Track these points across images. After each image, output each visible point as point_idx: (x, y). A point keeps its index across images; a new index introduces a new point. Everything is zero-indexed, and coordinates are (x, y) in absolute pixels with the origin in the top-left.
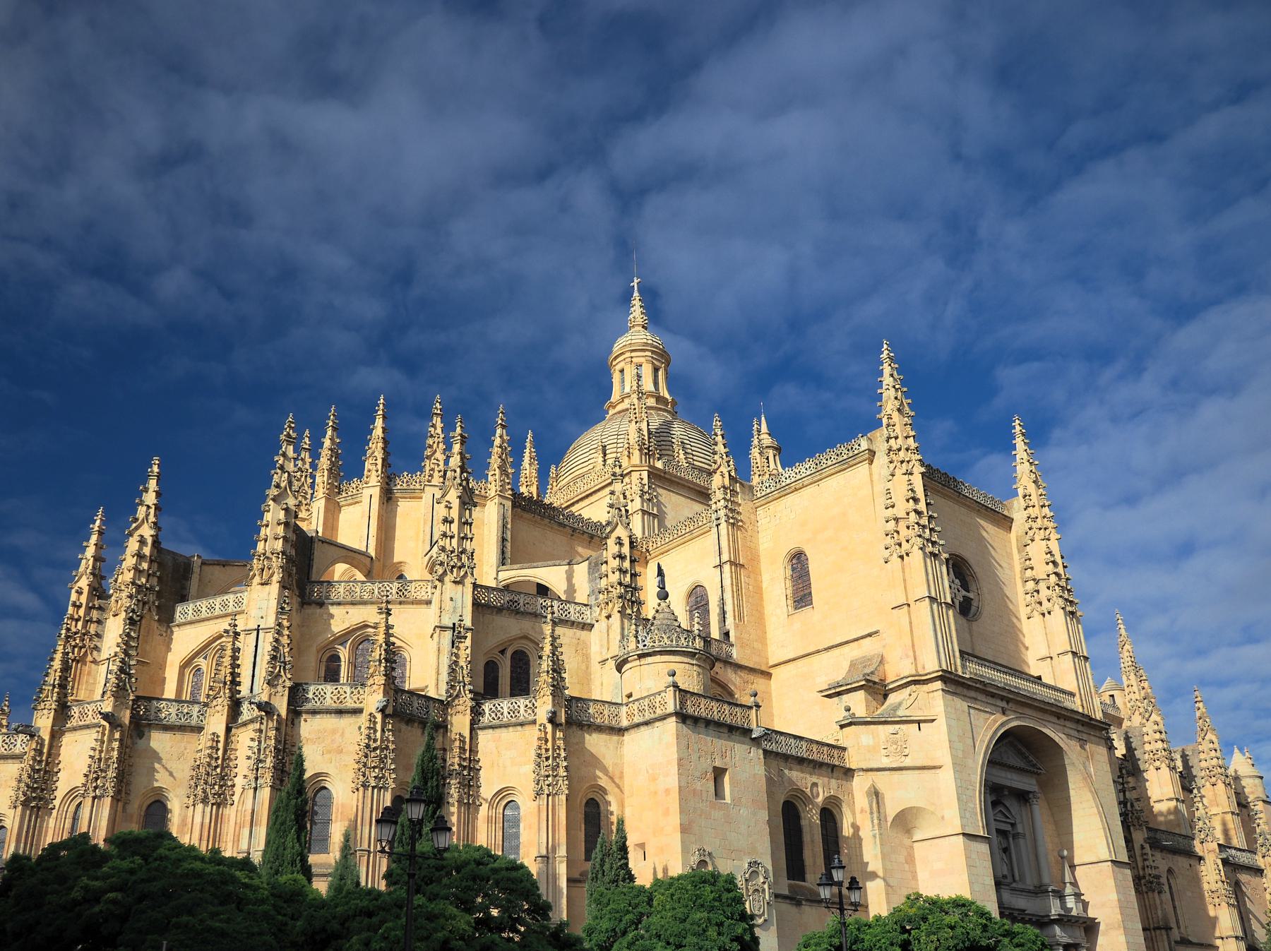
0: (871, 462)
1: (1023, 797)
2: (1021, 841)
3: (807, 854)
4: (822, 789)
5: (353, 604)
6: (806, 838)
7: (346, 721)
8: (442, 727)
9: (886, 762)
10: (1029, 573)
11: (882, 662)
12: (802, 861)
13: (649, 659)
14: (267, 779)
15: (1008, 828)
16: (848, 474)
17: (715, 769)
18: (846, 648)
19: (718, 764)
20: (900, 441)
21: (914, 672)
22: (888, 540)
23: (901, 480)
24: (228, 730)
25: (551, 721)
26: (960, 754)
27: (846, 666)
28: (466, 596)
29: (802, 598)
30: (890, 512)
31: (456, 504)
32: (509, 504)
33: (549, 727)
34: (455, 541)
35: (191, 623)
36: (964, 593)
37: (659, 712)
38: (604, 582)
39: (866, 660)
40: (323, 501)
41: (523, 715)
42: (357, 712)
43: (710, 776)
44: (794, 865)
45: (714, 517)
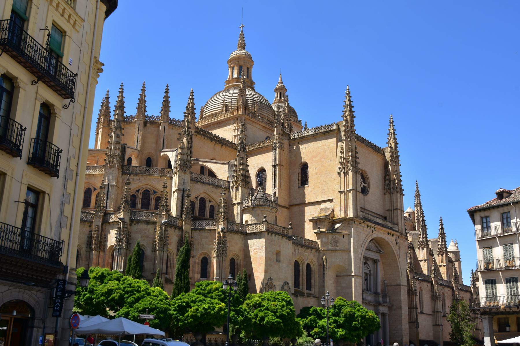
1: (375, 261)
2: (372, 277)
3: (301, 279)
4: (308, 257)
6: (301, 273)
7: (150, 227)
8: (181, 229)
9: (330, 248)
10: (387, 177)
11: (333, 211)
12: (299, 281)
13: (256, 209)
15: (368, 272)
17: (277, 250)
19: (278, 249)
21: (343, 216)
22: (340, 166)
24: (102, 224)
25: (222, 231)
26: (356, 247)
27: (319, 210)
28: (187, 177)
32: (193, 132)
33: (222, 234)
34: (185, 157)
36: (364, 184)
37: (259, 230)
39: (325, 209)
43: (275, 252)
44: (297, 284)
45: (273, 146)
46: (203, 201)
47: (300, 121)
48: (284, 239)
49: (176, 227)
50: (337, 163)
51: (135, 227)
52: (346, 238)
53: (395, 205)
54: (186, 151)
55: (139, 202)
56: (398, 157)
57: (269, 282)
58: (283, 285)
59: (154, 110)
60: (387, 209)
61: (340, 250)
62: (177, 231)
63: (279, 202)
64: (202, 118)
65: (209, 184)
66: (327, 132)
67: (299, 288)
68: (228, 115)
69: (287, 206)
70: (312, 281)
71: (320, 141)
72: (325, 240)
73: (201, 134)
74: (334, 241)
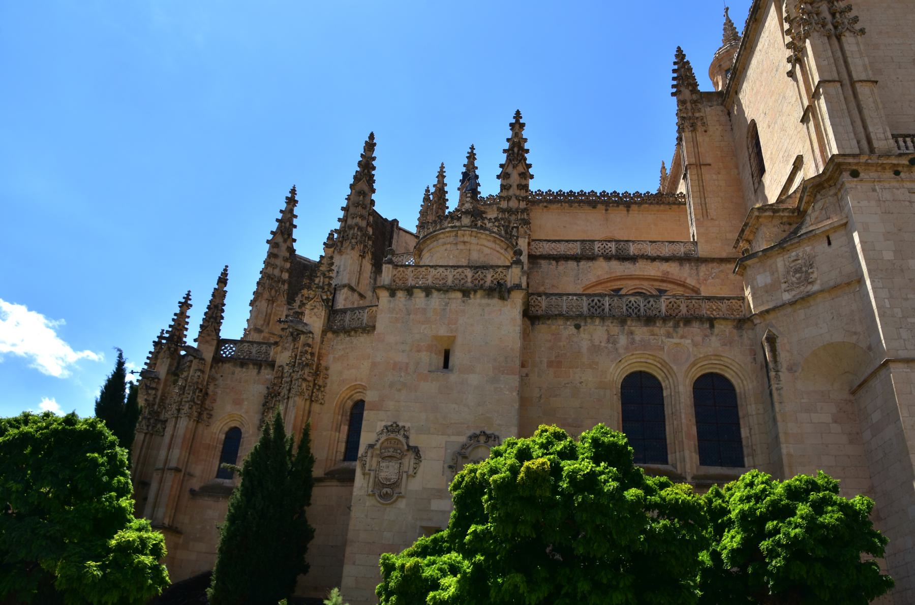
9: (787, 297)
19: (443, 332)
26: (888, 255)
29: (762, 170)
48: (478, 300)
50: (784, 48)
52: (838, 240)
57: (383, 437)
58: (464, 447)
61: (822, 291)
63: (703, 251)
67: (667, 463)
70: (744, 432)
71: (756, 46)
72: (763, 279)
73: (560, 201)
74: (797, 271)
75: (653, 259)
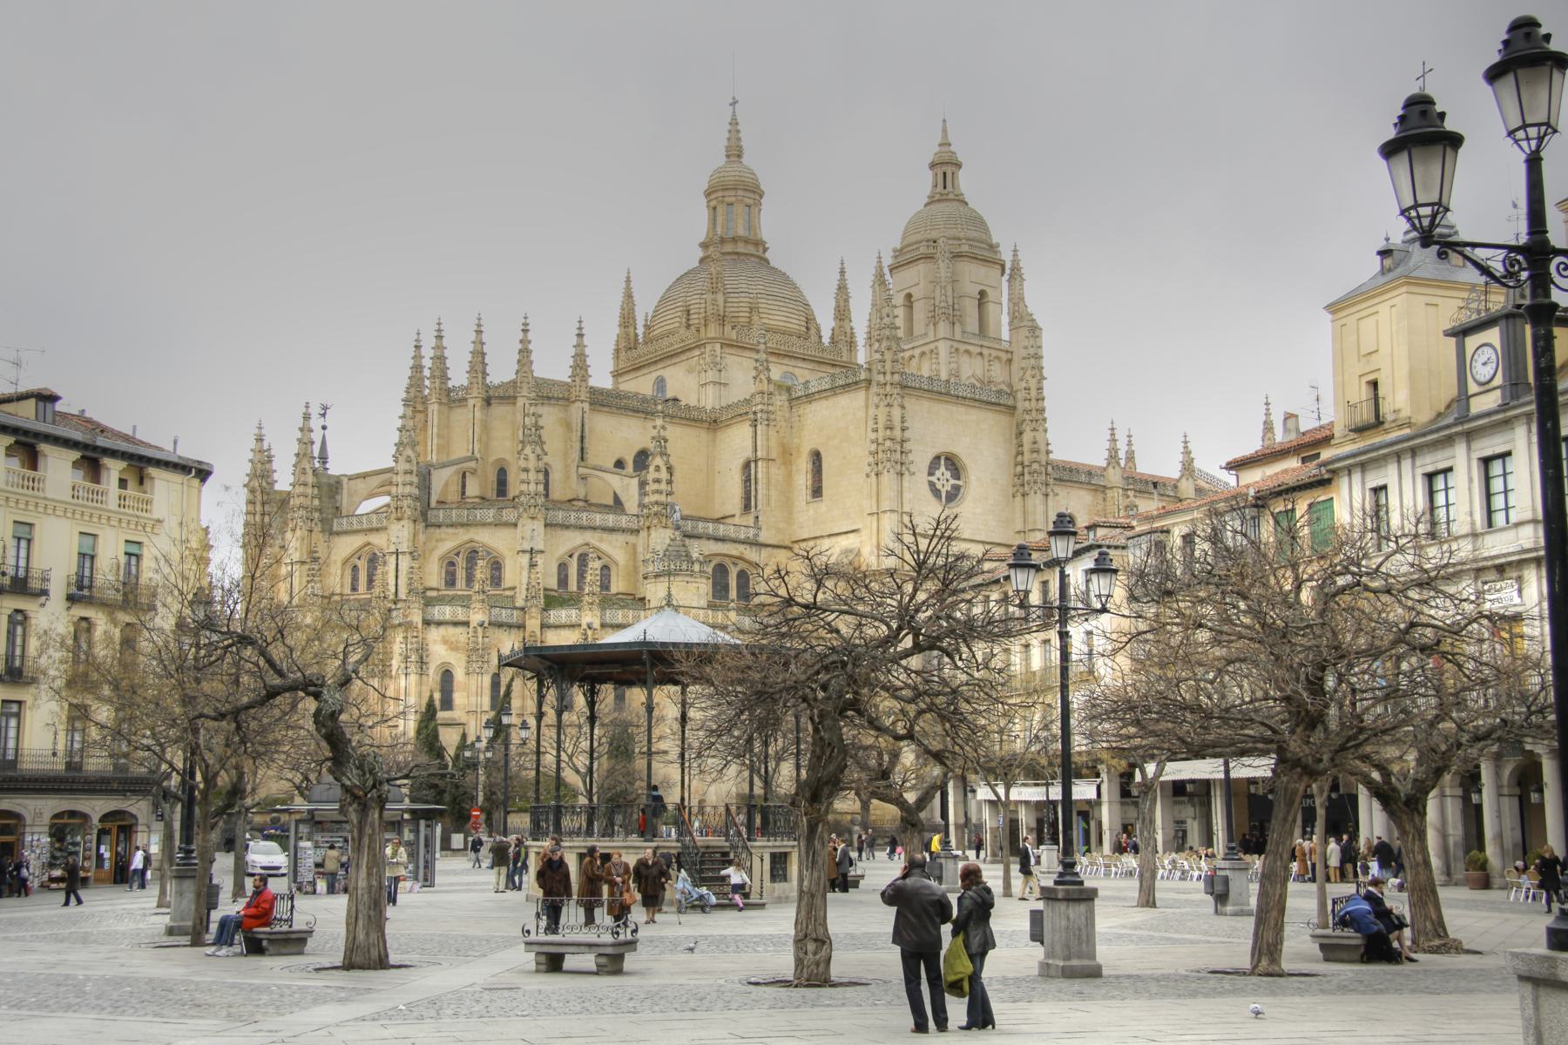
0: (868, 388)
5: (462, 525)
7: (460, 629)
8: (521, 627)
11: (859, 554)
14: (413, 668)
16: (852, 395)
18: (840, 538)
20: (888, 377)
22: (871, 459)
23: (882, 414)
29: (817, 492)
30: (873, 436)
31: (532, 457)
32: (586, 406)
35: (346, 533)
36: (953, 482)
38: (646, 500)
40: (436, 407)
41: (574, 620)
42: (466, 624)
46: (583, 561)
47: (998, 245)
49: (510, 626)
51: (434, 634)
53: (1030, 519)
54: (532, 476)
55: (461, 575)
56: (1042, 411)
59: (501, 371)
60: (1019, 527)
62: (514, 631)
64: (646, 343)
65: (594, 529)
66: (848, 385)
68: (689, 337)
69: (787, 543)
75: (734, 541)
